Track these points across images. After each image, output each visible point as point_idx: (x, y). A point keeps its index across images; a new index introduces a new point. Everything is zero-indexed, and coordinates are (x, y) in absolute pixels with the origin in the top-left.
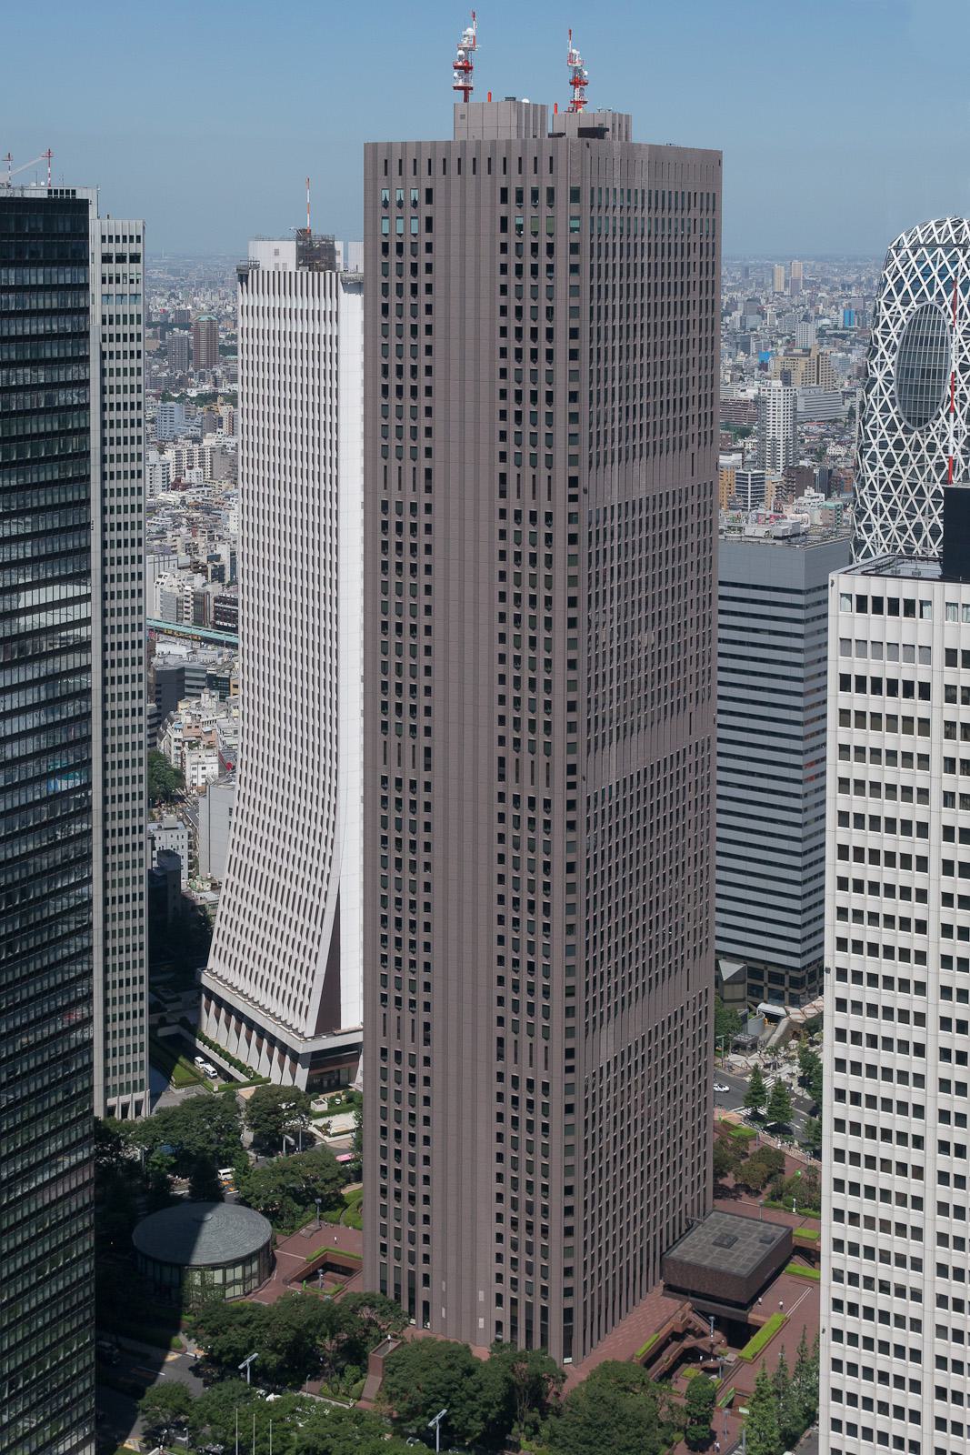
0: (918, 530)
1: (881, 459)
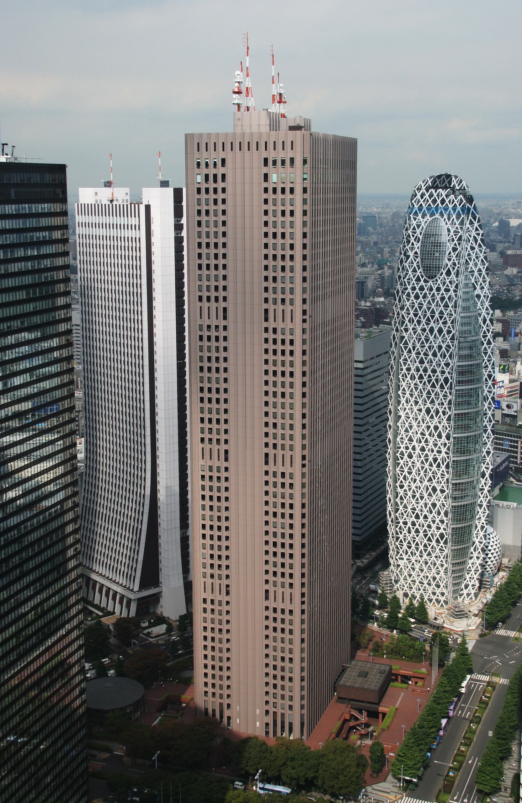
1: (412, 296)
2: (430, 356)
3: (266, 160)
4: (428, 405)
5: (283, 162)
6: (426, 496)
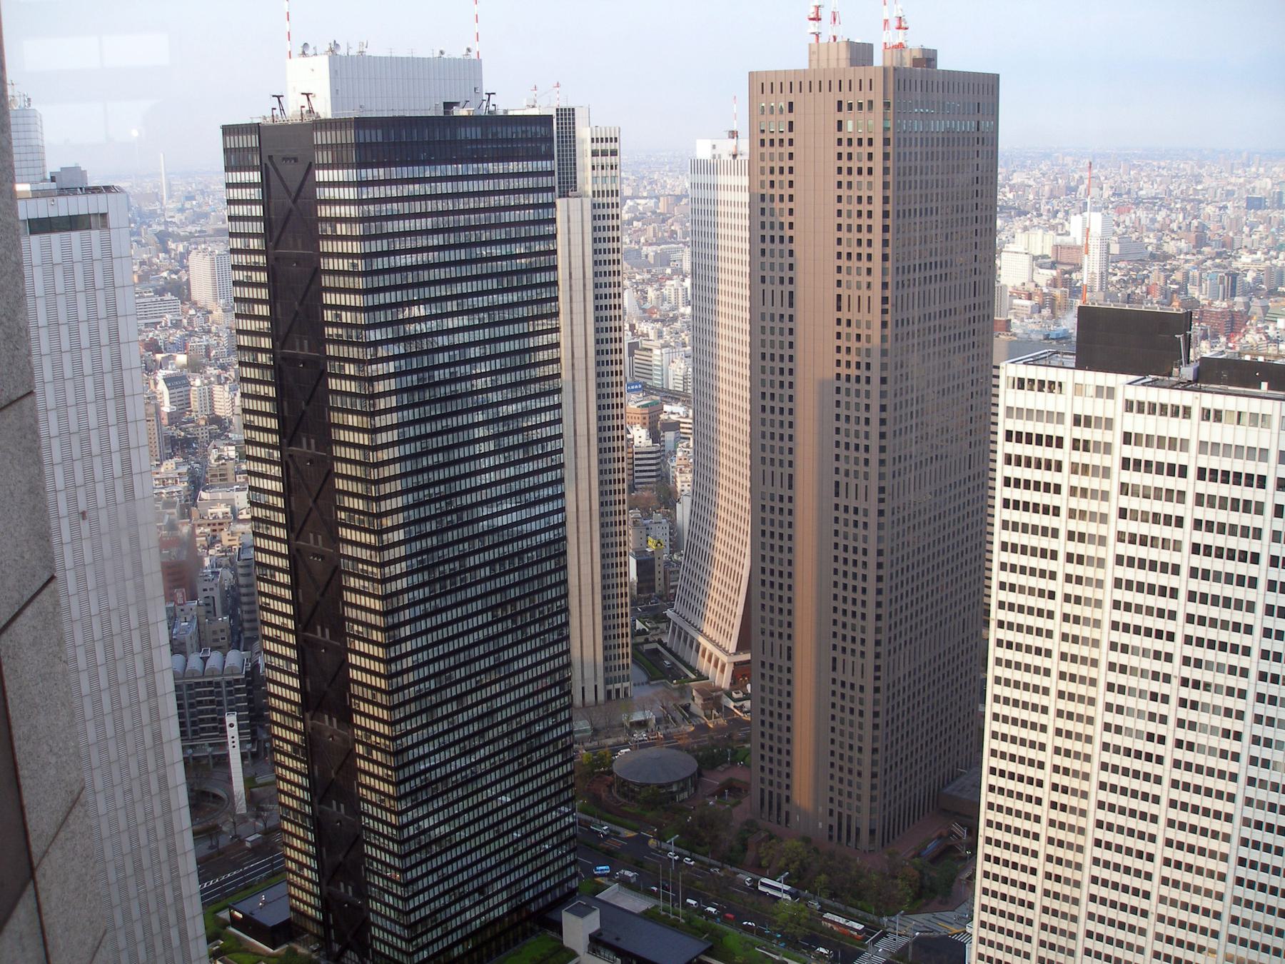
3: (840, 103)
5: (860, 105)
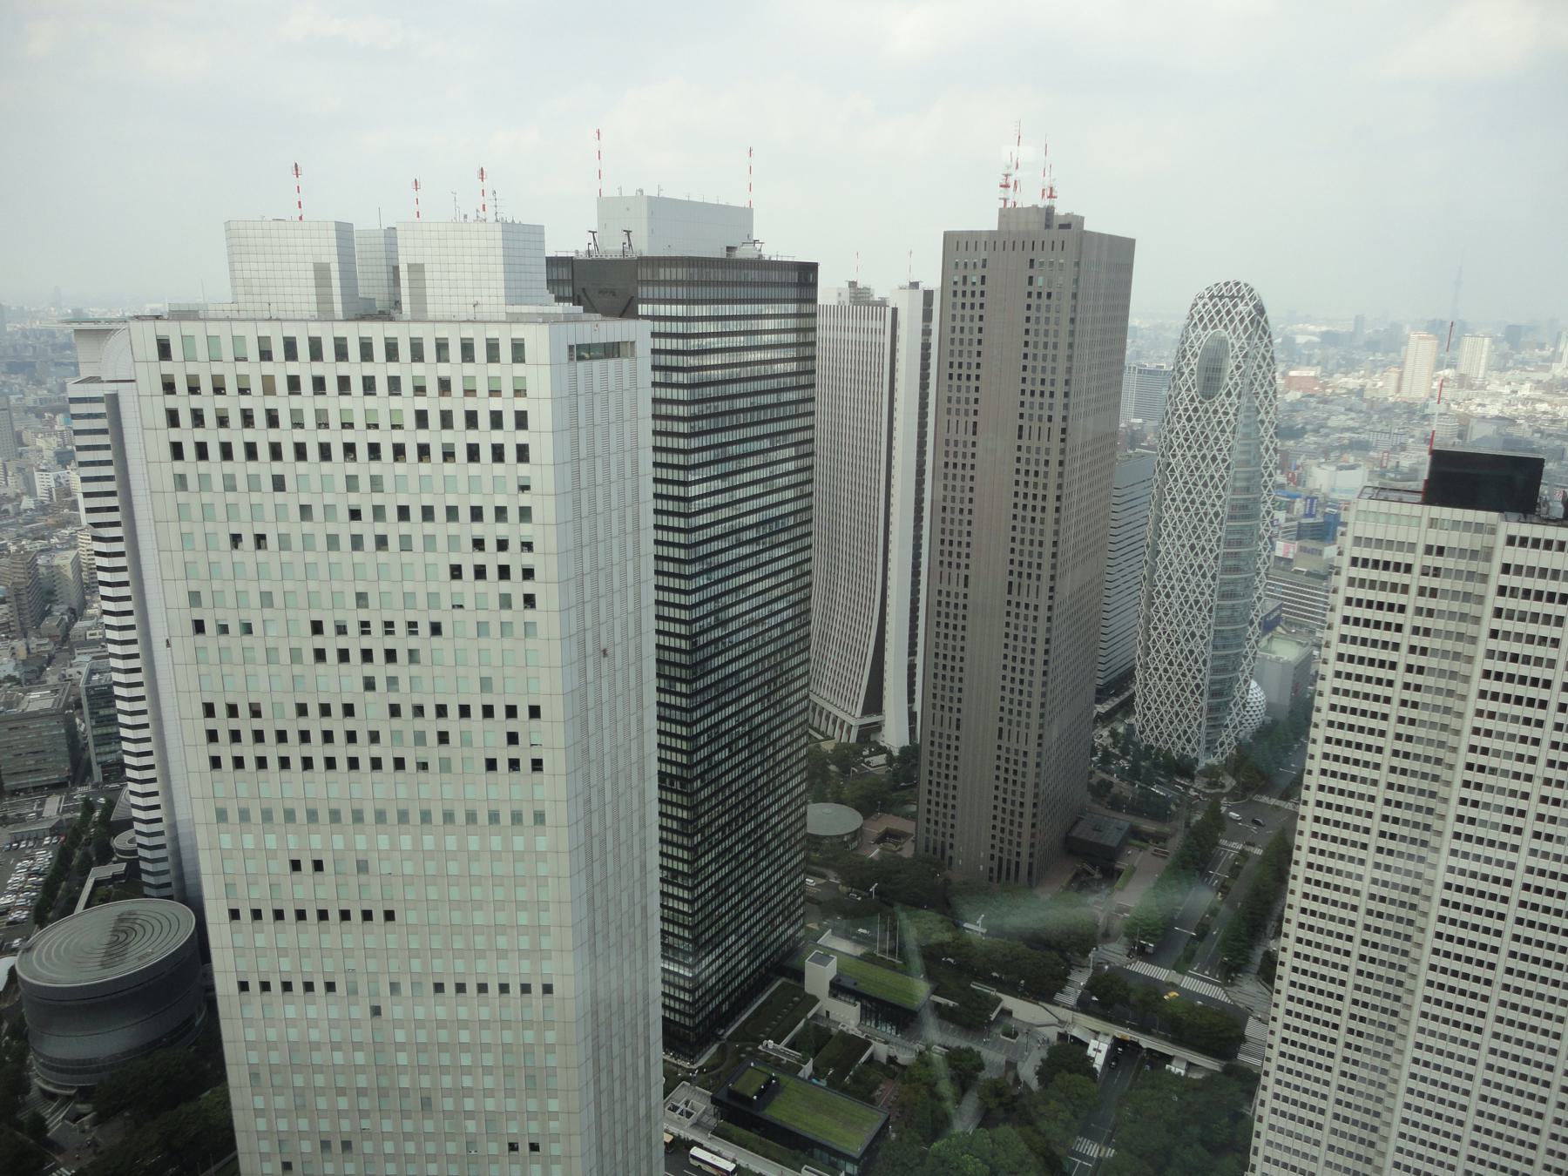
0: (1204, 458)
2: (1200, 487)
3: (1032, 261)
4: (1193, 540)
6: (1182, 641)
